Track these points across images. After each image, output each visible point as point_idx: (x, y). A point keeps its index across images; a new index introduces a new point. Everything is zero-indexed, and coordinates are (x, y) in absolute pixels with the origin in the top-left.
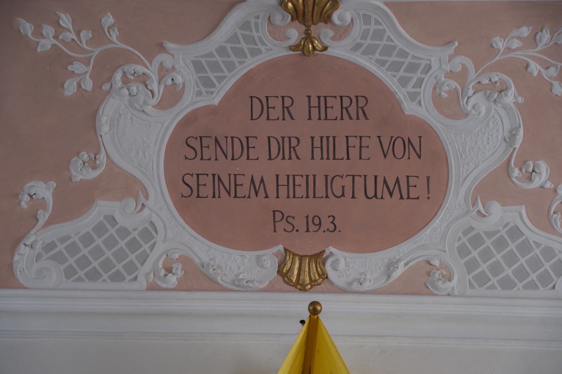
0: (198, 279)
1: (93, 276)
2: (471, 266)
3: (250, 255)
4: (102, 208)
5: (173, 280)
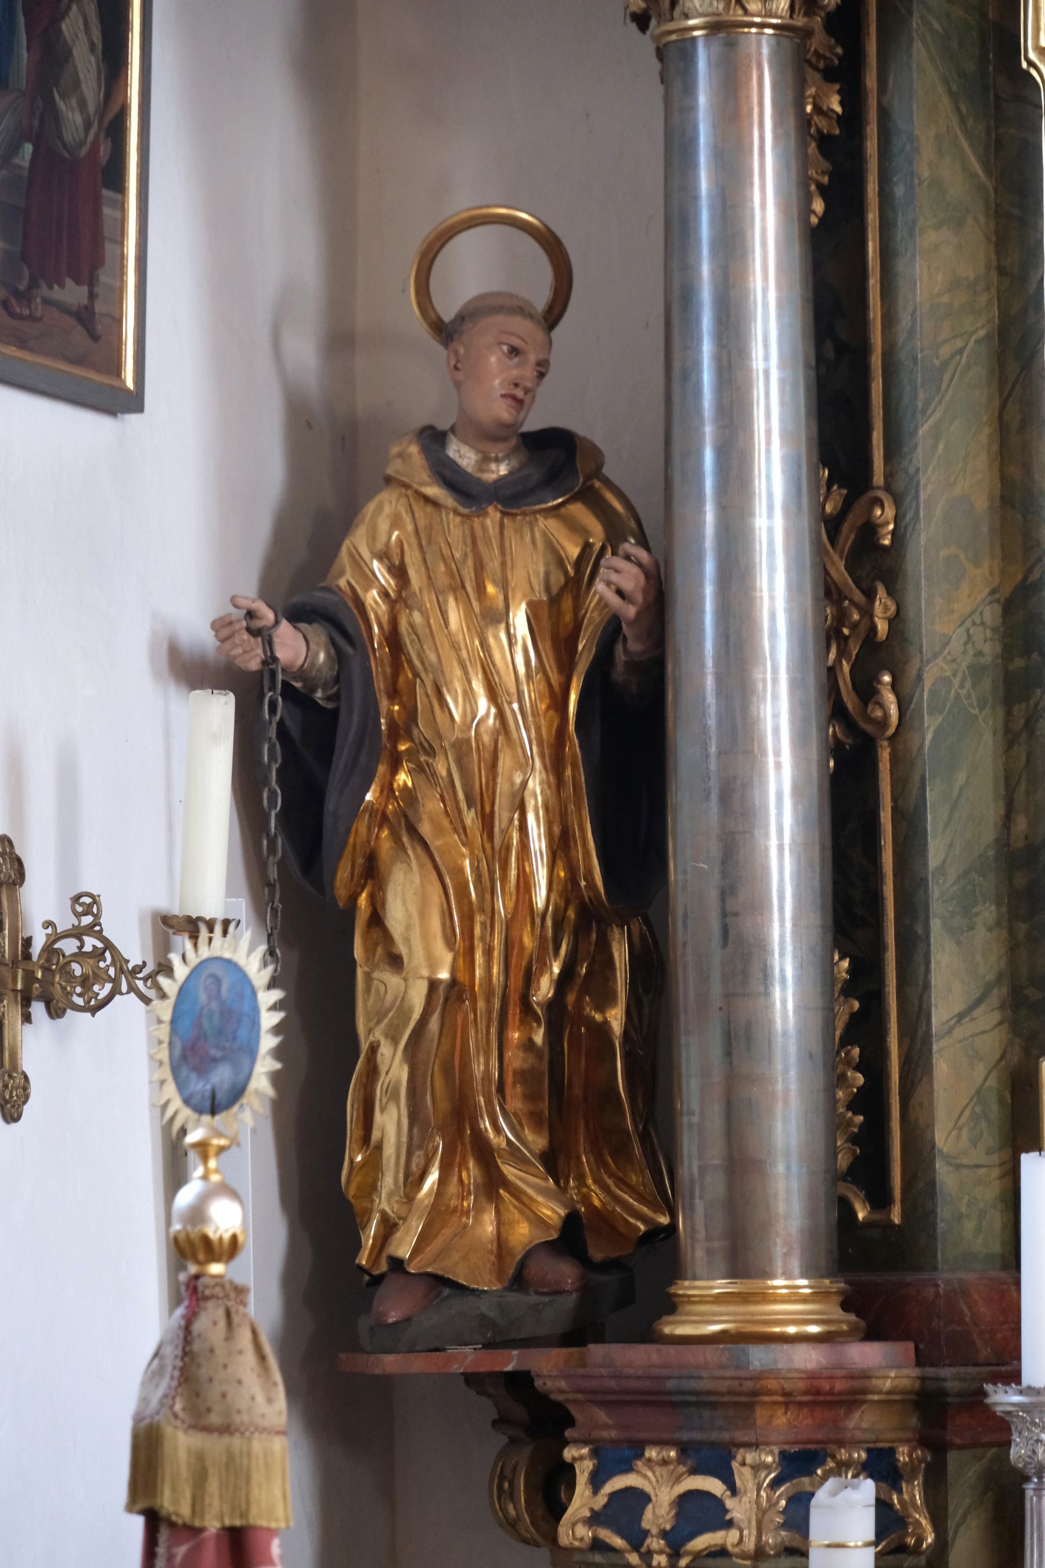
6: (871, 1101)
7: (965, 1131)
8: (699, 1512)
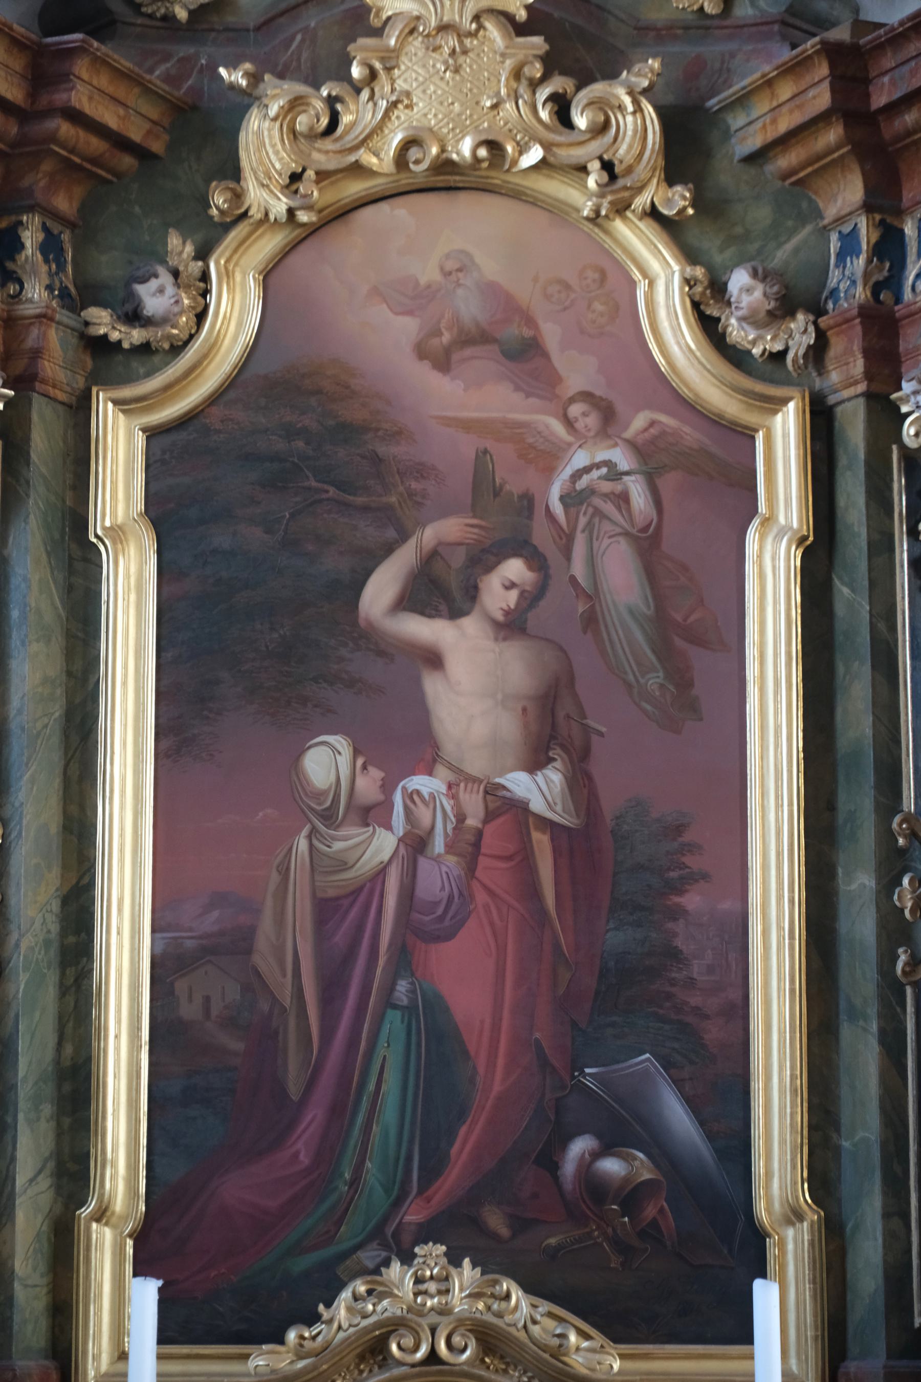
7: (30, 1261)
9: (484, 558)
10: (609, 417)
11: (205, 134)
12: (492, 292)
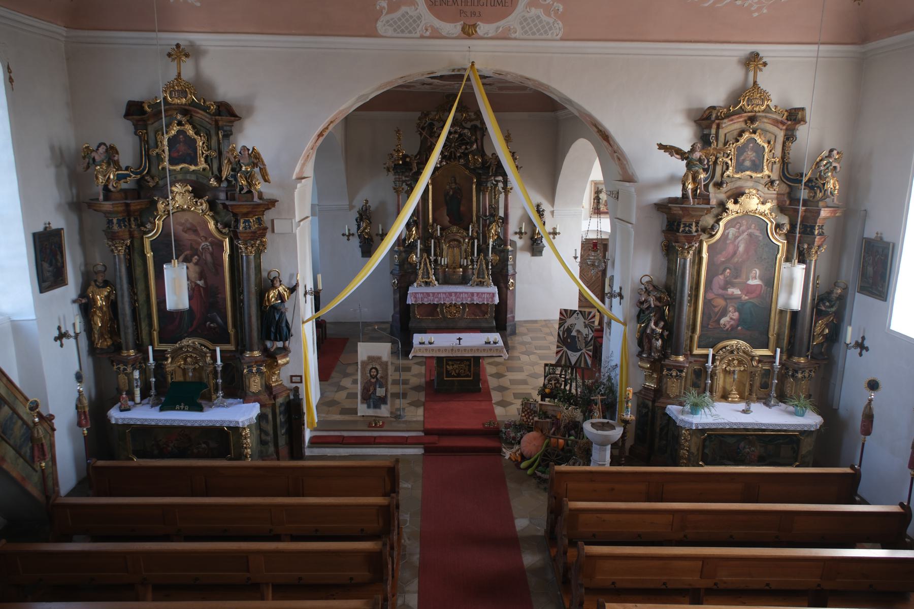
0: (436, 35)
1: (403, 31)
2: (523, 28)
3: (452, 25)
4: (404, 9)
5: (428, 34)
6: (137, 329)
8: (125, 369)
9: (192, 256)
10: (206, 239)
11: (154, 204)
12: (191, 223)
